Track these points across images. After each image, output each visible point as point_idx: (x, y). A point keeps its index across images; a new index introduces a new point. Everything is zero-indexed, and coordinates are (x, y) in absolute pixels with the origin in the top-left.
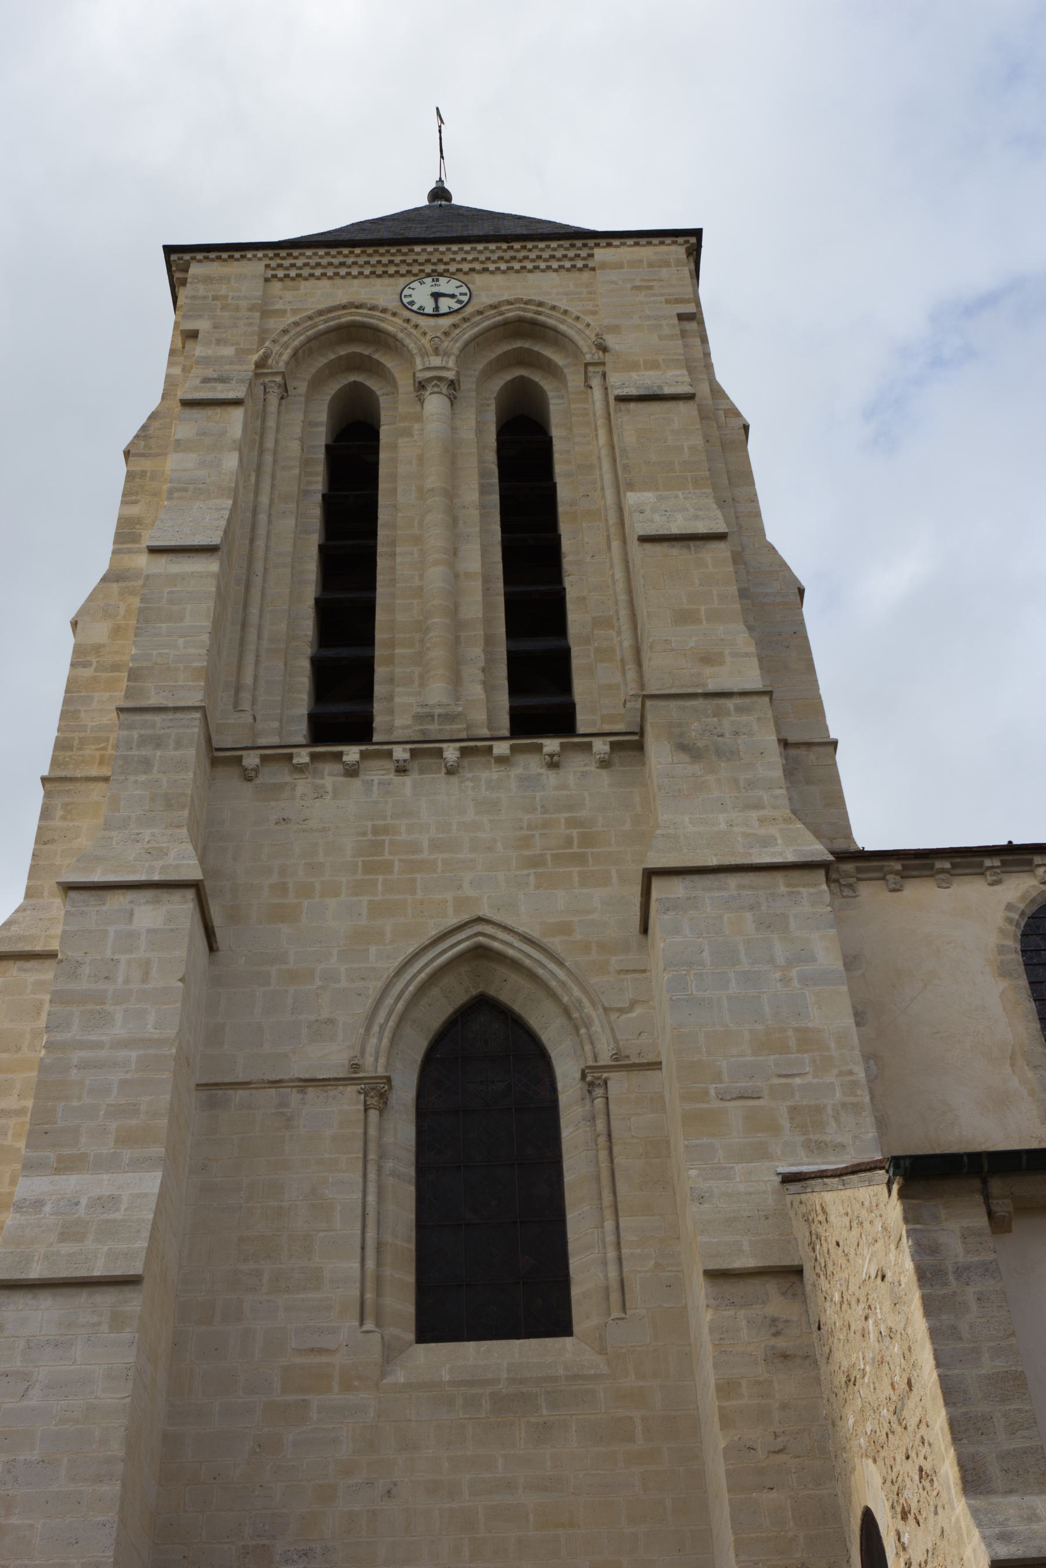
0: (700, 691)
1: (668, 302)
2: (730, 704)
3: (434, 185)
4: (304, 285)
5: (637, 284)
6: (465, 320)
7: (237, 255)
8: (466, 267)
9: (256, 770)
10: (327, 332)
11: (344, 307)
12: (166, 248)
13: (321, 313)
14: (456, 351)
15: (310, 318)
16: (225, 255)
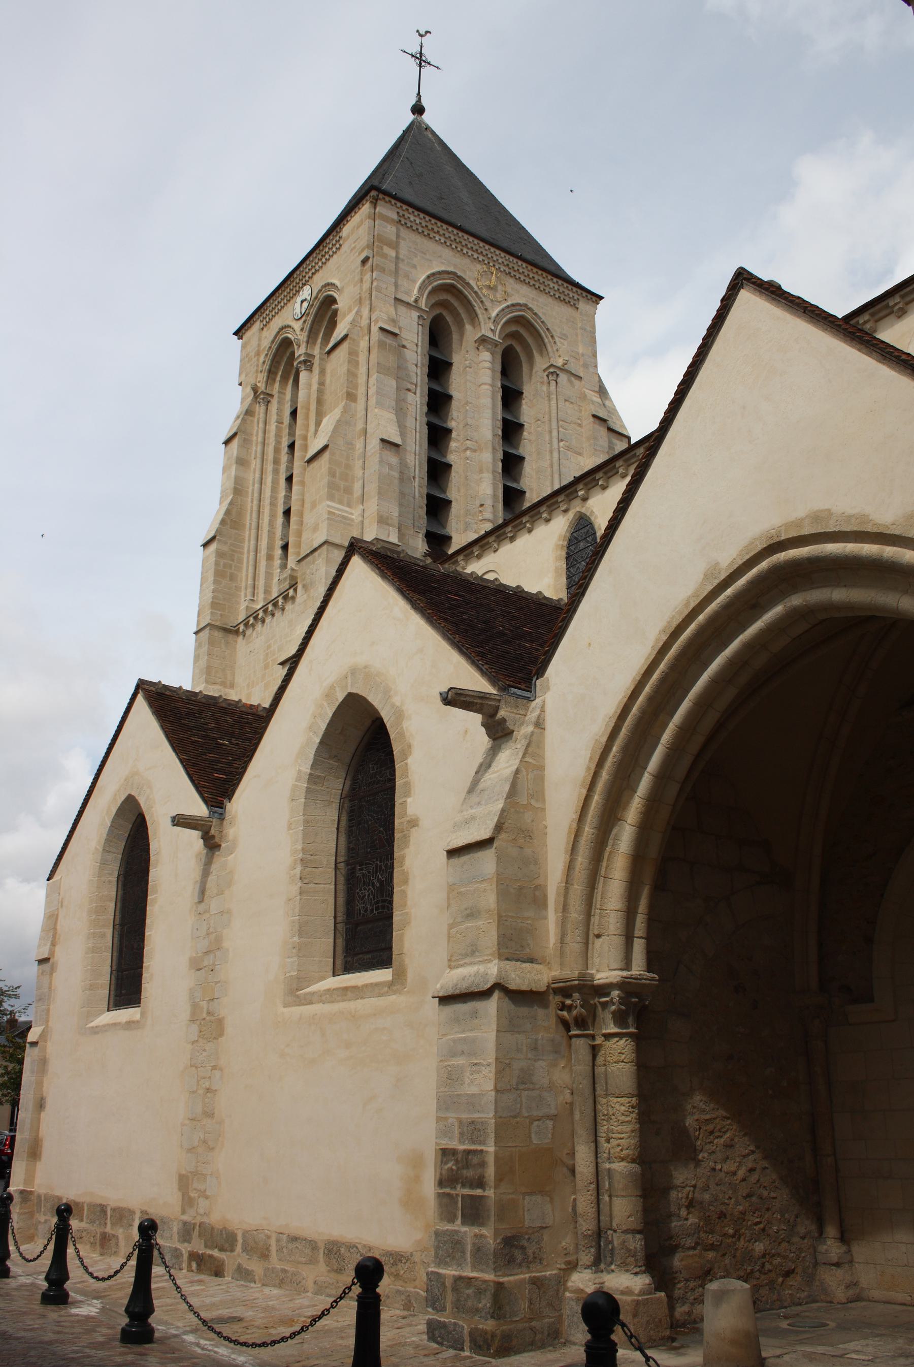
0: (309, 551)
1: (360, 254)
2: (316, 554)
3: (413, 102)
4: (272, 323)
5: (353, 245)
6: (308, 314)
7: (252, 322)
8: (310, 274)
9: (244, 631)
10: (278, 349)
11: (279, 332)
12: (236, 333)
13: (273, 342)
14: (305, 339)
15: (270, 347)
16: (249, 325)
